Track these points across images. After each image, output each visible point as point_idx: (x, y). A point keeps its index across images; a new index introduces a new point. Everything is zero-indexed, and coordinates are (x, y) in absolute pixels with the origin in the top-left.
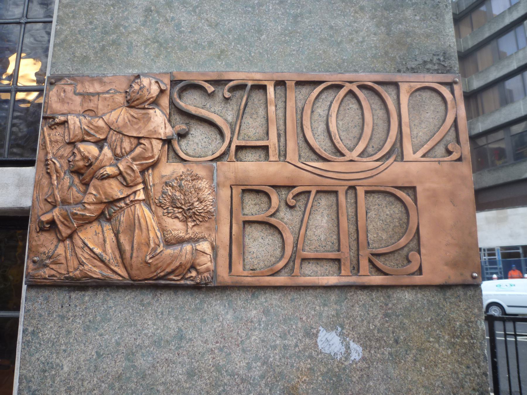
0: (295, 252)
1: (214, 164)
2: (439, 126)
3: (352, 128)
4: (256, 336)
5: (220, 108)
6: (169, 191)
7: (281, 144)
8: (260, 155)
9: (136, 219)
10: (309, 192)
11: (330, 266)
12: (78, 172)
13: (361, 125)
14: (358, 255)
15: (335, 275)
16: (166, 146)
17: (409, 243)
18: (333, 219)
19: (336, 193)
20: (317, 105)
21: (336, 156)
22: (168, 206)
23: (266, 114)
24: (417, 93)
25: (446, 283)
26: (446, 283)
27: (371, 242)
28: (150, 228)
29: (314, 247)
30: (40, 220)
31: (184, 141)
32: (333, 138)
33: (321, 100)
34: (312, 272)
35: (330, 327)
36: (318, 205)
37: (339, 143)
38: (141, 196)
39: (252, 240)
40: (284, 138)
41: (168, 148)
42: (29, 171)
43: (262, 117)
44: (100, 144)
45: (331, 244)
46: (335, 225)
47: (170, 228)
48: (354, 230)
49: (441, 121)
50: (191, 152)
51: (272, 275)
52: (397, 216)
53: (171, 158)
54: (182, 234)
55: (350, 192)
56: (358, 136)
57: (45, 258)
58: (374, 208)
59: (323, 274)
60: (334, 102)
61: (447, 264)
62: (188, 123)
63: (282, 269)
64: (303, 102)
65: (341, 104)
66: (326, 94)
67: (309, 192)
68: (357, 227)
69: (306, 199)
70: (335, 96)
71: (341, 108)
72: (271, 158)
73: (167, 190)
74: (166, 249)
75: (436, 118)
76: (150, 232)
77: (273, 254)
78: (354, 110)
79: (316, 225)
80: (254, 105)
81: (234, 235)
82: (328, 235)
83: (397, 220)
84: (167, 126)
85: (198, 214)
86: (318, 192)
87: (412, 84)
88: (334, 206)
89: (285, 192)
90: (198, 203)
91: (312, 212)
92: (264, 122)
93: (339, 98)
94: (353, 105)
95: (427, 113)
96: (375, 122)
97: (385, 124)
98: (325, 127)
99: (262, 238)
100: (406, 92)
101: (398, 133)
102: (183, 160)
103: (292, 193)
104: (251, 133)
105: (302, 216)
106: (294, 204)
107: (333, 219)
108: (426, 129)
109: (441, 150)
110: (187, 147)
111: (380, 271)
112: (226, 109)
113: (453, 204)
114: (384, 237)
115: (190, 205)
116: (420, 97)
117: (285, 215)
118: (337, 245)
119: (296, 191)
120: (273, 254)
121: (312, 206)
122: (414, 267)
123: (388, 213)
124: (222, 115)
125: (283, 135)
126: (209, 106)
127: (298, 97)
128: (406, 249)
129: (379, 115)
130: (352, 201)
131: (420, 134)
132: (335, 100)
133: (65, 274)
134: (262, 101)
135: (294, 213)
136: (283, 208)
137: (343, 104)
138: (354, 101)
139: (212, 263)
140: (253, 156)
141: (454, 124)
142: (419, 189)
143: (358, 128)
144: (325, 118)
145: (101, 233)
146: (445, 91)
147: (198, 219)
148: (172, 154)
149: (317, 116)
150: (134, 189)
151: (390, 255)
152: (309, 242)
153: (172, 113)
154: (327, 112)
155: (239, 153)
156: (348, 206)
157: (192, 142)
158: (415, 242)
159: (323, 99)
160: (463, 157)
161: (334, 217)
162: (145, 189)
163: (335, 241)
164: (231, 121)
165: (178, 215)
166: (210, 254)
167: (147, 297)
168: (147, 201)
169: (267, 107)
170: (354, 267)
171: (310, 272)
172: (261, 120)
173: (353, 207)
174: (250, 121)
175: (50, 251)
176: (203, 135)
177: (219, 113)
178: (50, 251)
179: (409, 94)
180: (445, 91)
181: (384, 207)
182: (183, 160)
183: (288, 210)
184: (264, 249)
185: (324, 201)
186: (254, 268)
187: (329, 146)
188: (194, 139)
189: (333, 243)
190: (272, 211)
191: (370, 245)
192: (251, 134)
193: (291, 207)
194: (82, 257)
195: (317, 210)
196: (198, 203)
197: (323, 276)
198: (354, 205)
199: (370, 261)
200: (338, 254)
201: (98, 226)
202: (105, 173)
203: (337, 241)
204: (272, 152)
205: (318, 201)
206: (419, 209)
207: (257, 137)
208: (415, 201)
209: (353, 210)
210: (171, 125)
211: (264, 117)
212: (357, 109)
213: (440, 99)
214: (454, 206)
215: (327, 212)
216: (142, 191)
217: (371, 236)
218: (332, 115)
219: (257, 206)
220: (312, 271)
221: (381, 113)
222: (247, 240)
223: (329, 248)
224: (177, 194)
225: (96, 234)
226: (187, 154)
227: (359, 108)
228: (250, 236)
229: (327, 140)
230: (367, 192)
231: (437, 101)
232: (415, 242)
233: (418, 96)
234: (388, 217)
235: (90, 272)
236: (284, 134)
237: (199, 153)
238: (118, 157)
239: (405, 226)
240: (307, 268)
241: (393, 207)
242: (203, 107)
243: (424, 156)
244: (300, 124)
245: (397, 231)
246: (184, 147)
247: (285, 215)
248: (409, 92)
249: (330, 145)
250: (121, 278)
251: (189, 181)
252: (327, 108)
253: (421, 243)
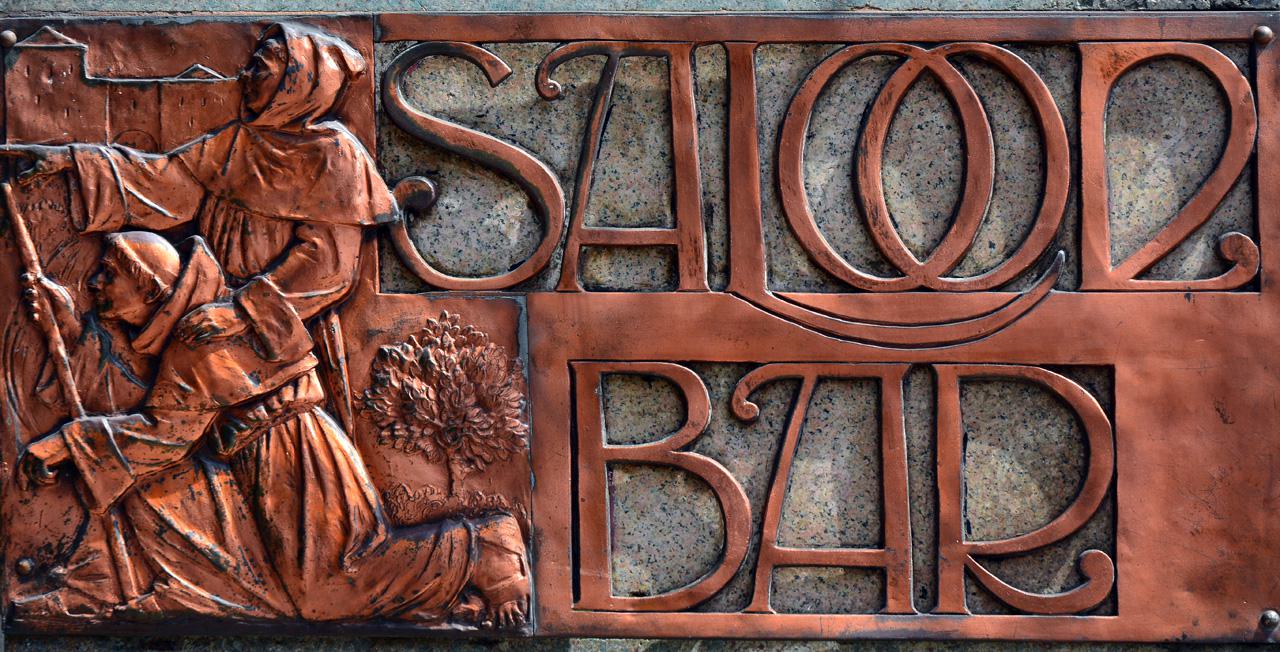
0: (759, 545)
1: (521, 300)
2: (1200, 179)
3: (931, 187)
5: (529, 126)
6: (392, 376)
7: (713, 238)
8: (652, 271)
9: (307, 455)
10: (798, 381)
11: (855, 586)
13: (956, 177)
14: (936, 556)
15: (871, 610)
16: (376, 244)
17: (1084, 526)
18: (866, 458)
19: (876, 383)
20: (824, 115)
21: (880, 273)
22: (392, 420)
23: (667, 145)
24: (1139, 75)
25: (1184, 636)
26: (1184, 636)
27: (975, 522)
28: (348, 479)
29: (812, 535)
30: (28, 454)
31: (425, 227)
32: (870, 221)
33: (837, 99)
34: (804, 603)
36: (825, 415)
37: (886, 235)
38: (313, 389)
39: (633, 514)
40: (724, 219)
41: (380, 249)
43: (656, 152)
45: (859, 526)
46: (872, 474)
47: (401, 478)
48: (926, 489)
49: (1208, 162)
50: (448, 261)
51: (694, 609)
52: (1055, 449)
53: (390, 278)
54: (438, 496)
55: (918, 379)
56: (946, 212)
57: (51, 561)
58: (987, 425)
59: (835, 609)
60: (876, 106)
61: (1190, 586)
62: (436, 172)
63: (720, 591)
64: (780, 104)
65: (897, 110)
66: (852, 79)
67: (798, 381)
68: (935, 479)
69: (788, 400)
70: (882, 86)
71: (899, 125)
72: (686, 282)
73: (387, 373)
74: (396, 537)
75: (1194, 155)
76: (347, 491)
77: (693, 551)
78: (938, 129)
79: (818, 473)
80: (632, 115)
81: (583, 500)
82: (850, 500)
83: (1053, 462)
84: (373, 184)
85: (478, 440)
86: (821, 380)
87: (1122, 47)
88: (871, 419)
89: (727, 380)
90: (477, 410)
91: (806, 435)
92: (663, 170)
93: (890, 95)
94: (934, 116)
95: (1167, 137)
96: (1002, 166)
97: (1033, 176)
98: (848, 185)
99: (664, 509)
100: (1100, 74)
101: (1069, 200)
102: (424, 286)
103: (748, 384)
104: (626, 203)
105: (775, 447)
106: (752, 415)
107: (866, 458)
108: (1160, 190)
109: (1196, 257)
110: (436, 247)
111: (998, 604)
112: (547, 128)
113: (1222, 416)
114: (1013, 511)
115: (452, 405)
116: (1147, 87)
117: (727, 443)
118: (876, 529)
119: (757, 376)
120: (693, 551)
121: (806, 420)
122: (1096, 593)
123: (1030, 440)
124: (536, 147)
125: (719, 211)
126: (494, 118)
127: (766, 89)
128: (1077, 543)
129: (1014, 145)
130: (924, 406)
131: (1141, 204)
132: (877, 102)
133: (115, 605)
134: (654, 104)
135: (753, 438)
136: (722, 424)
137: (905, 112)
138: (936, 100)
139: (523, 573)
140: (632, 273)
141: (1248, 171)
142: (1124, 373)
143: (950, 186)
144: (848, 156)
145: (205, 493)
146: (1226, 66)
147: (480, 457)
148: (392, 266)
149: (825, 149)
150: (293, 370)
151: (1030, 557)
152: (797, 520)
153: (386, 139)
154: (853, 136)
155: (589, 263)
156: (911, 420)
157: (449, 232)
158: (1104, 522)
159: (843, 96)
160: (1263, 278)
161: (869, 452)
162: (326, 371)
163: (870, 517)
164: (563, 165)
165: (422, 444)
166: (518, 551)
168: (332, 404)
169: (669, 122)
170: (924, 591)
171: (801, 602)
172: (652, 163)
173: (925, 423)
174: (620, 165)
175: (64, 541)
176: (481, 207)
177: (526, 140)
178: (64, 541)
179: (1110, 81)
180: (1226, 66)
181: (1016, 424)
182: (424, 286)
183: (736, 430)
184: (668, 538)
185: (845, 408)
186: (643, 589)
187: (860, 243)
188: (455, 221)
189: (865, 525)
190: (688, 433)
191: (973, 530)
192: (625, 207)
193: (747, 424)
194: (157, 559)
195: (820, 431)
196: (477, 410)
197: (837, 613)
198: (929, 417)
199: (969, 573)
200: (877, 554)
201: (196, 472)
202: (205, 324)
203: (876, 518)
204: (686, 263)
205: (824, 406)
206: (1117, 431)
207: (643, 216)
208: (1110, 410)
209: (926, 432)
210: (383, 177)
211: (663, 154)
212: (949, 127)
213: (1210, 91)
214: (1225, 421)
215: (851, 437)
216: (314, 374)
217: (978, 506)
218: (870, 148)
219: (648, 418)
220: (804, 599)
221: (1019, 139)
222: (622, 513)
223: (855, 536)
224: (416, 384)
225: (193, 495)
226: (436, 266)
227: (953, 123)
228: (629, 503)
229: (853, 225)
230: (965, 382)
231: (1199, 99)
232: (1103, 525)
233: (1141, 83)
234: (1028, 452)
235: (186, 599)
236: (722, 205)
237: (472, 264)
239: (1076, 477)
240: (790, 592)
241: (1046, 422)
242: (478, 120)
243: (1142, 274)
244: (770, 175)
245: (1052, 492)
246: (426, 246)
247: (727, 443)
248: (1108, 75)
249: (863, 239)
250: (271, 616)
251: (450, 346)
252: (854, 124)
253: (1119, 527)
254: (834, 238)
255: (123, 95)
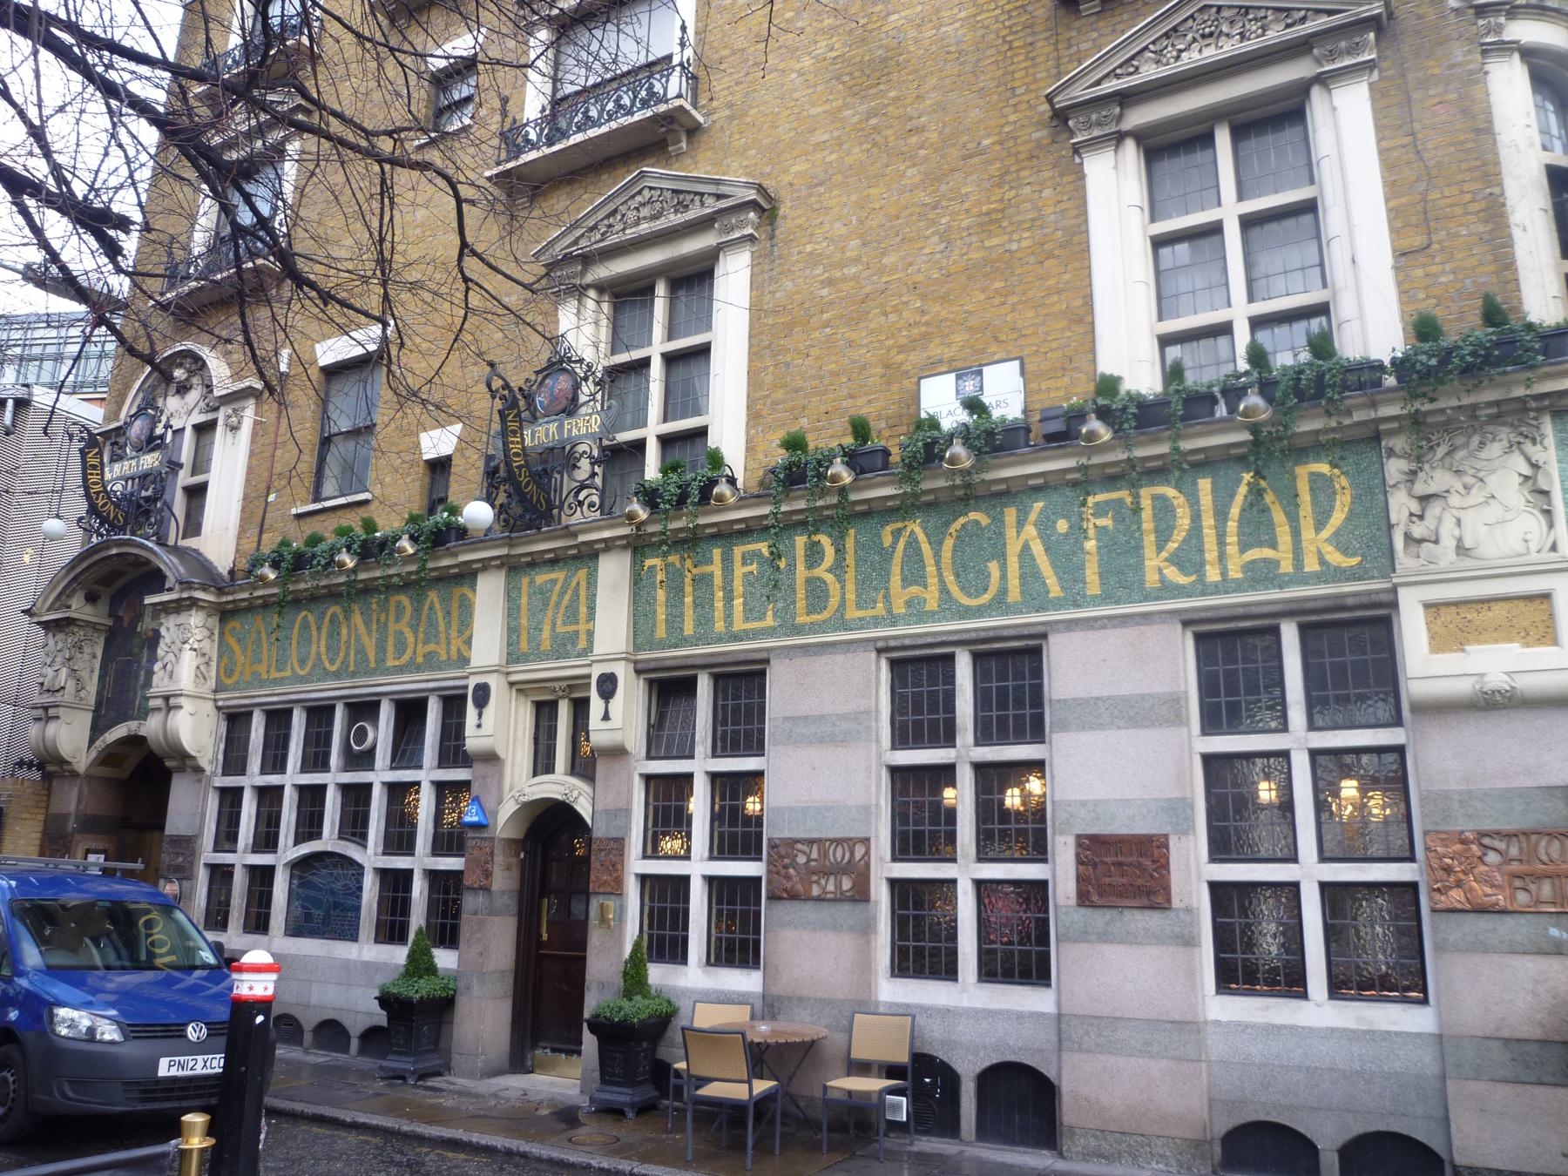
4: (1525, 929)
12: (1444, 870)
35: (1554, 926)
42: (1414, 865)
44: (1452, 859)
167: (1479, 915)
238: (1460, 864)
254: (1544, 857)
255: (1442, 840)
